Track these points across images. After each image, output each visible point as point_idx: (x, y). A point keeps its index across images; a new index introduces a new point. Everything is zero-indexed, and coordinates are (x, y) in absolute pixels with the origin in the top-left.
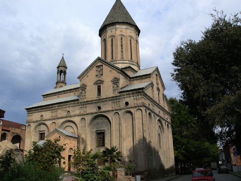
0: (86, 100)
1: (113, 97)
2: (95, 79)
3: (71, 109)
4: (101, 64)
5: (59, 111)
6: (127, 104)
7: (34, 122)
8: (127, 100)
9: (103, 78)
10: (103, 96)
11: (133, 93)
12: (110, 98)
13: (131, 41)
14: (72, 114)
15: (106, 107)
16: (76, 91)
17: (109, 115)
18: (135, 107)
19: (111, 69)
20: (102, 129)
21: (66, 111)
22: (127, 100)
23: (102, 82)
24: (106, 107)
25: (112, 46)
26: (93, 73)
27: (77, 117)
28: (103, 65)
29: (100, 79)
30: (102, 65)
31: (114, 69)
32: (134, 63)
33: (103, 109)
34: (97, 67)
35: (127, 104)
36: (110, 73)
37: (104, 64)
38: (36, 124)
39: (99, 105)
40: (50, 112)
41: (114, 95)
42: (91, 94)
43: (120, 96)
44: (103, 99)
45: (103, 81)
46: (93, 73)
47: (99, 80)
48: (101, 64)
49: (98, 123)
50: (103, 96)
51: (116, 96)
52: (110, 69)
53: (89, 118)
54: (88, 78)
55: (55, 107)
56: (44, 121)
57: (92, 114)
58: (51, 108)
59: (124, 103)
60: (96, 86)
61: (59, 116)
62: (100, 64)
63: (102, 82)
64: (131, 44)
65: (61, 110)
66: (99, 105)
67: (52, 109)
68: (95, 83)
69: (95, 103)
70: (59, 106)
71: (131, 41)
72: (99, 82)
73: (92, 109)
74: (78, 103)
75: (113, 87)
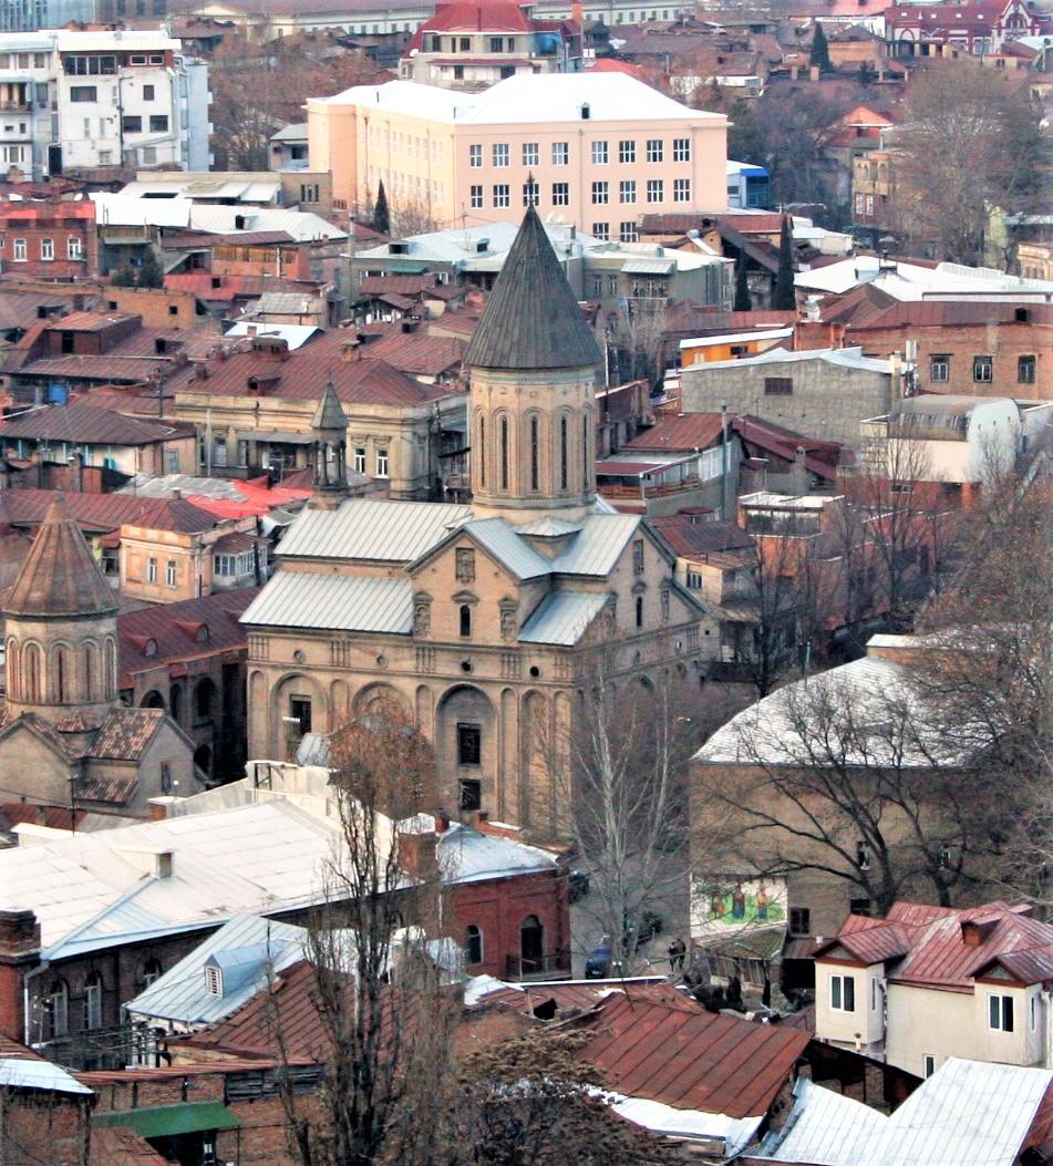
1: (504, 648)
2: (458, 587)
3: (388, 653)
5: (354, 652)
6: (535, 671)
7: (274, 667)
9: (477, 588)
11: (548, 650)
12: (491, 647)
13: (564, 422)
14: (392, 666)
18: (555, 686)
20: (474, 721)
21: (373, 653)
22: (536, 662)
23: (476, 600)
24: (485, 669)
26: (448, 562)
27: (407, 680)
29: (468, 587)
32: (571, 501)
34: (458, 549)
35: (535, 671)
38: (281, 674)
40: (324, 646)
41: (502, 644)
42: (444, 626)
43: (518, 649)
45: (478, 600)
46: (448, 562)
47: (463, 593)
49: (463, 705)
51: (510, 648)
52: (495, 569)
54: (435, 575)
56: (308, 669)
57: (449, 679)
59: (529, 668)
62: (464, 544)
63: (476, 600)
64: (564, 434)
66: (465, 658)
68: (457, 597)
69: (459, 651)
70: (350, 637)
71: (564, 422)
72: (464, 597)
73: (448, 668)
75: (503, 622)
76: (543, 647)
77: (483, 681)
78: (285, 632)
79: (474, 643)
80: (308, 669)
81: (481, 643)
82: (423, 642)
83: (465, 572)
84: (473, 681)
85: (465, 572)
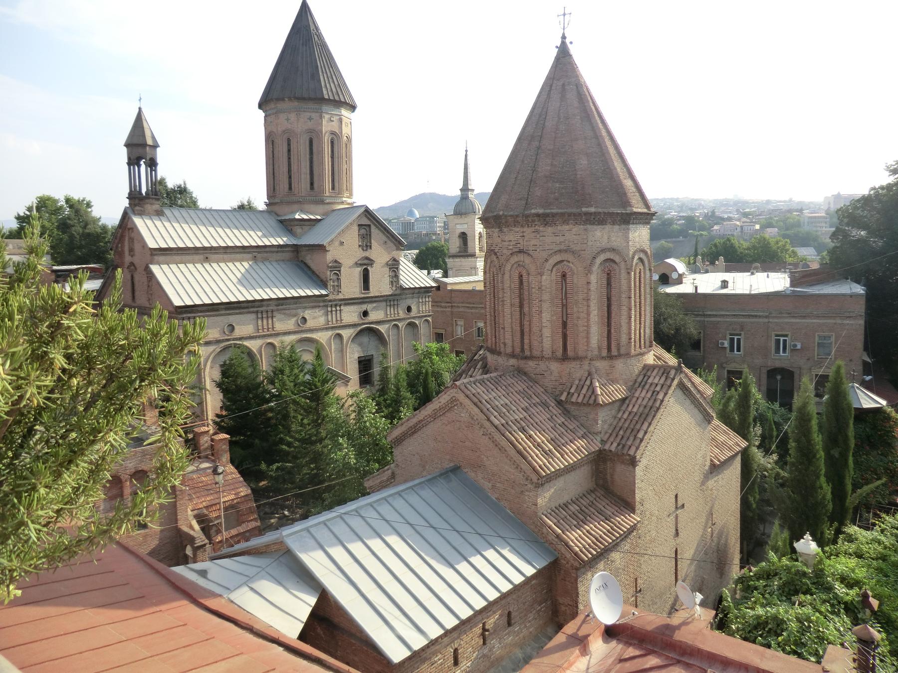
0: (341, 296)
3: (308, 314)
4: (368, 222)
7: (207, 343)
8: (409, 302)
10: (374, 291)
14: (310, 324)
16: (259, 252)
17: (382, 328)
25: (332, 157)
28: (373, 227)
29: (366, 254)
30: (369, 226)
31: (391, 241)
33: (374, 316)
37: (375, 225)
39: (364, 307)
40: (253, 316)
43: (400, 295)
44: (372, 297)
50: (374, 291)
52: (384, 238)
53: (346, 333)
55: (268, 306)
57: (354, 326)
58: (259, 307)
60: (358, 270)
65: (284, 314)
67: (261, 309)
74: (324, 301)
76: (416, 291)
77: (379, 322)
78: (217, 310)
79: (371, 295)
80: (241, 339)
81: (377, 294)
82: (335, 300)
84: (372, 323)
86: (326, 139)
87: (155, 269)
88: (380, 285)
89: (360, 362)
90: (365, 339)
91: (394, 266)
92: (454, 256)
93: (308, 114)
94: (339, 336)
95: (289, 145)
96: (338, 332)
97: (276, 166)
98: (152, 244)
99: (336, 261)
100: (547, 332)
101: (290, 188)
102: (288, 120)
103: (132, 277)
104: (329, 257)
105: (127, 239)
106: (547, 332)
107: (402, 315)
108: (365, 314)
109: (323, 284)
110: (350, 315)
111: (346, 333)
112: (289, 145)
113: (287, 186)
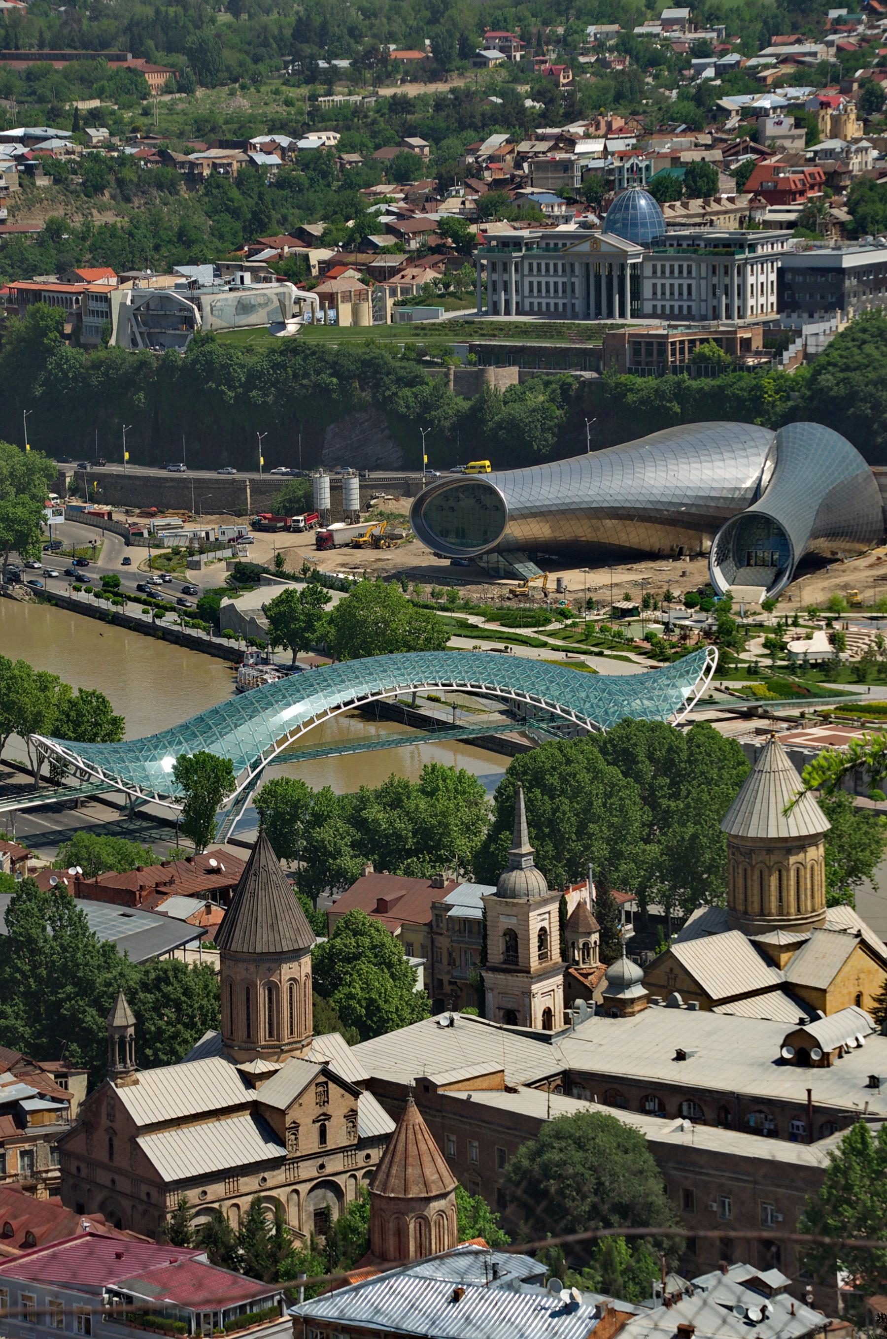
0: (298, 1154)
3: (266, 1175)
9: (330, 1109)
14: (270, 1183)
15: (334, 1164)
19: (343, 1092)
23: (328, 1117)
25: (291, 1004)
30: (326, 1083)
33: (329, 1169)
34: (317, 1085)
36: (341, 1100)
39: (320, 1161)
48: (325, 1079)
50: (330, 1145)
53: (304, 1188)
61: (243, 1190)
63: (328, 1117)
83: (324, 1099)
85: (324, 1099)
86: (285, 986)
87: (140, 1141)
88: (338, 1136)
89: (316, 1215)
90: (320, 1192)
91: (352, 1116)
92: (494, 969)
93: (267, 965)
94: (297, 1192)
95: (248, 993)
96: (294, 1187)
97: (234, 1012)
98: (139, 1123)
99: (294, 1122)
100: (392, 1249)
101: (249, 1036)
102: (247, 970)
103: (111, 1140)
104: (288, 1120)
105: (105, 1104)
106: (392, 1249)
107: (361, 1164)
108: (322, 1166)
109: (282, 1143)
110: (308, 1170)
111: (304, 1188)
112: (248, 993)
113: (246, 1033)
